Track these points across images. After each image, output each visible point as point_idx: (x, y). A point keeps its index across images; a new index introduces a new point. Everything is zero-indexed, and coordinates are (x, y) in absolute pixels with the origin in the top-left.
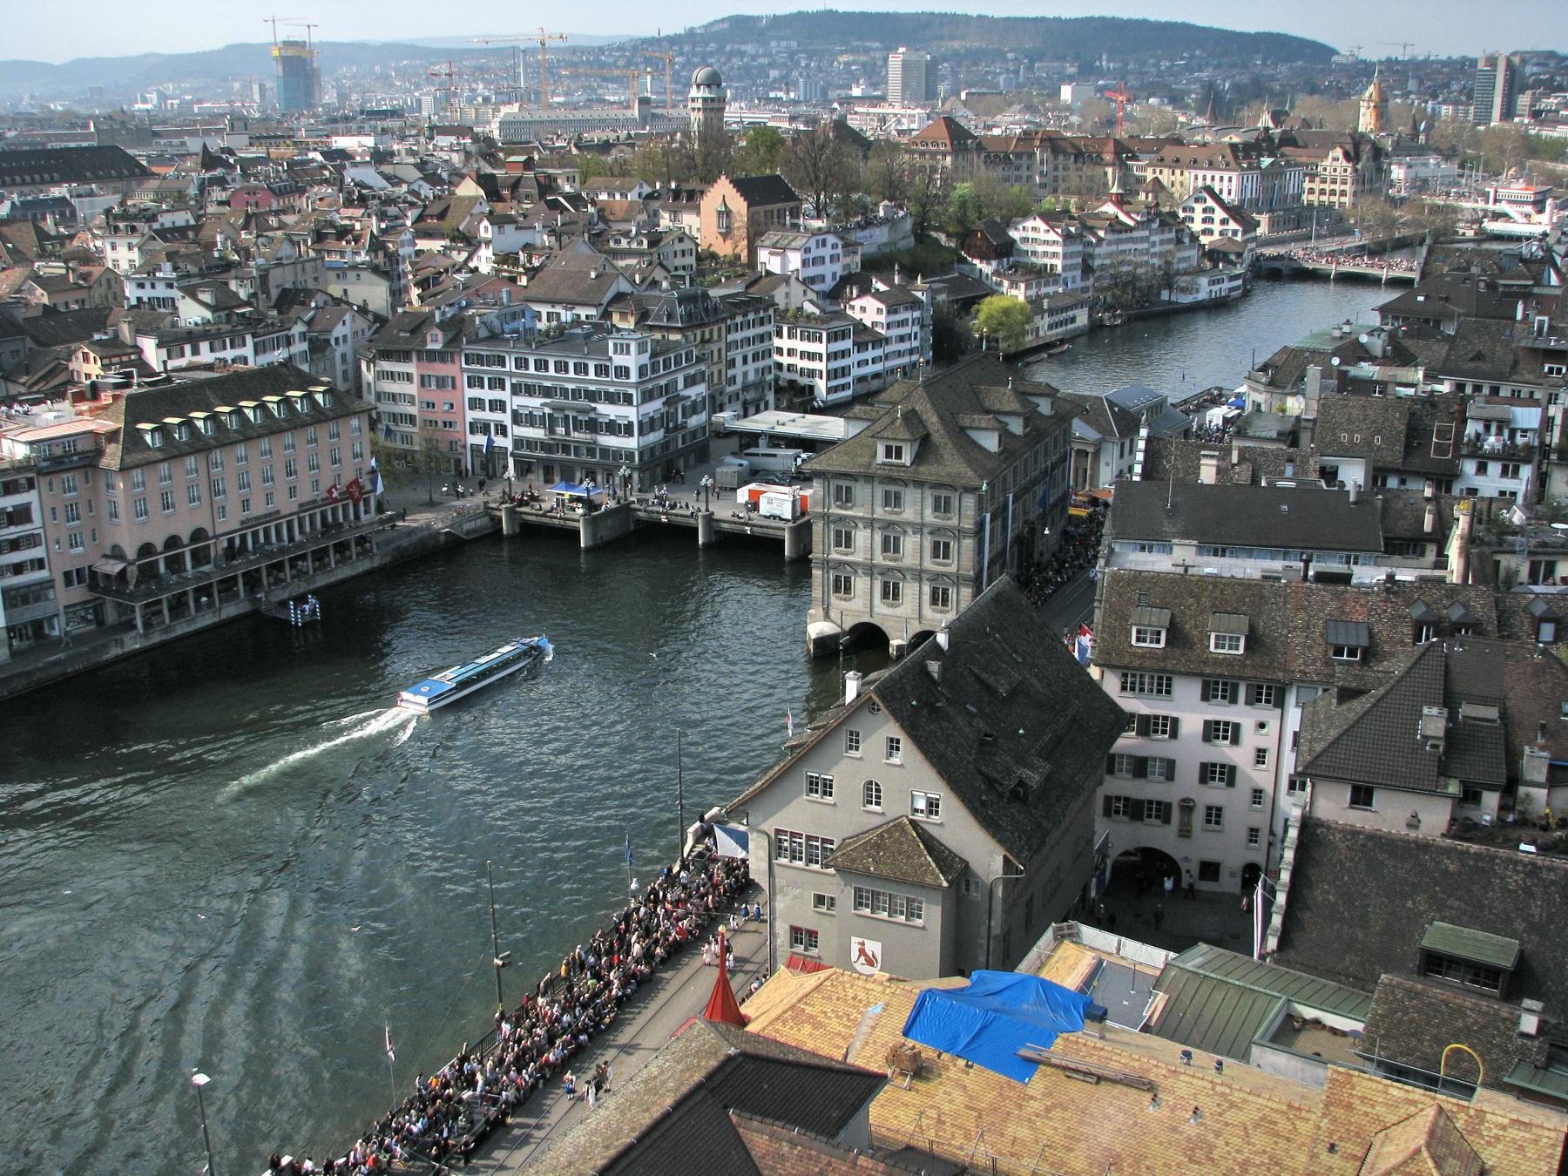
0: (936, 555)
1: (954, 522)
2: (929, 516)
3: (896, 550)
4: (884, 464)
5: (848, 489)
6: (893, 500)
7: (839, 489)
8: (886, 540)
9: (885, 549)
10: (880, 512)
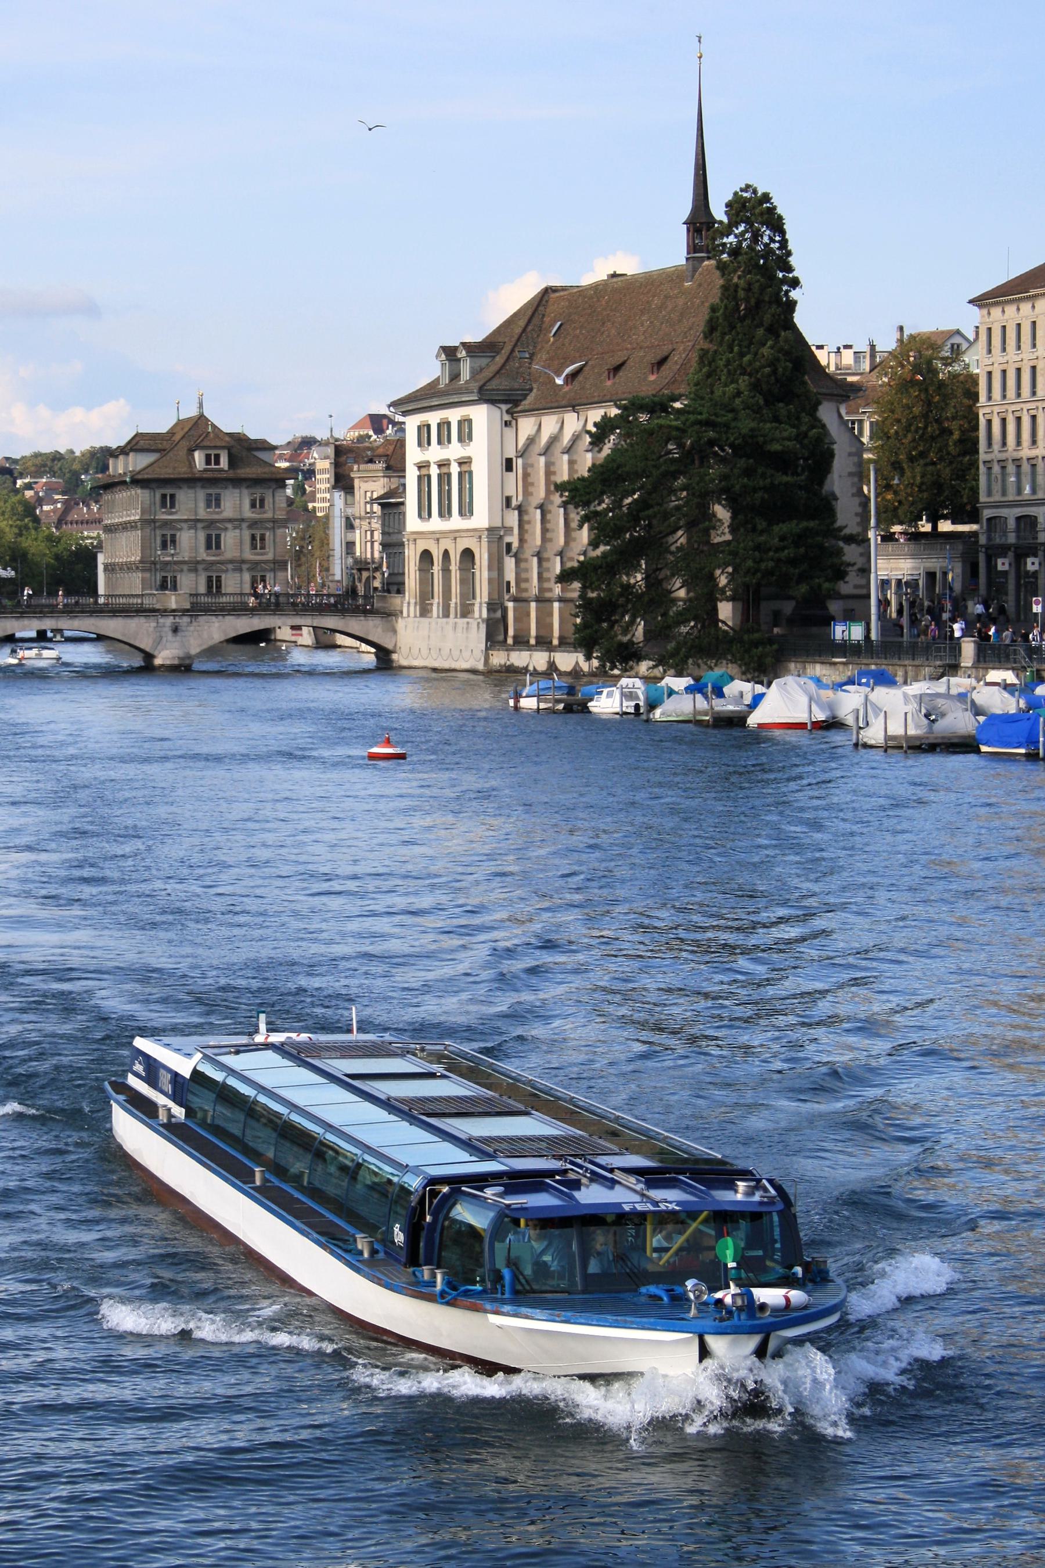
0: (254, 547)
1: (269, 515)
2: (248, 513)
3: (218, 547)
4: (205, 470)
5: (172, 496)
6: (214, 501)
7: (164, 496)
8: (209, 538)
9: (209, 547)
10: (202, 513)
